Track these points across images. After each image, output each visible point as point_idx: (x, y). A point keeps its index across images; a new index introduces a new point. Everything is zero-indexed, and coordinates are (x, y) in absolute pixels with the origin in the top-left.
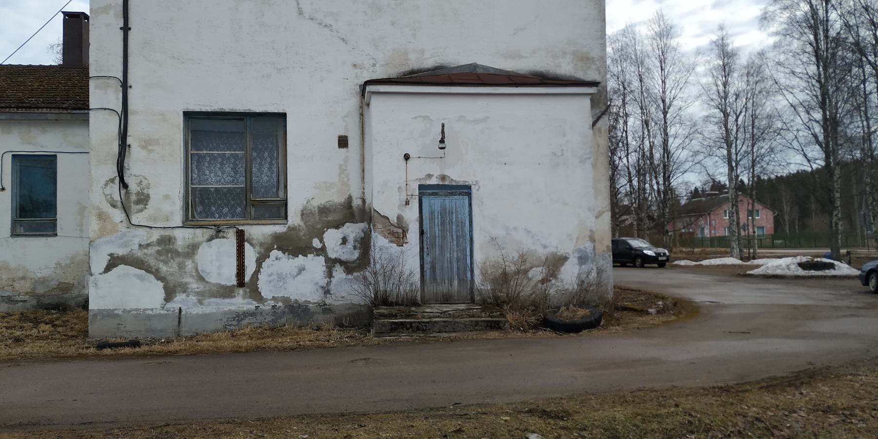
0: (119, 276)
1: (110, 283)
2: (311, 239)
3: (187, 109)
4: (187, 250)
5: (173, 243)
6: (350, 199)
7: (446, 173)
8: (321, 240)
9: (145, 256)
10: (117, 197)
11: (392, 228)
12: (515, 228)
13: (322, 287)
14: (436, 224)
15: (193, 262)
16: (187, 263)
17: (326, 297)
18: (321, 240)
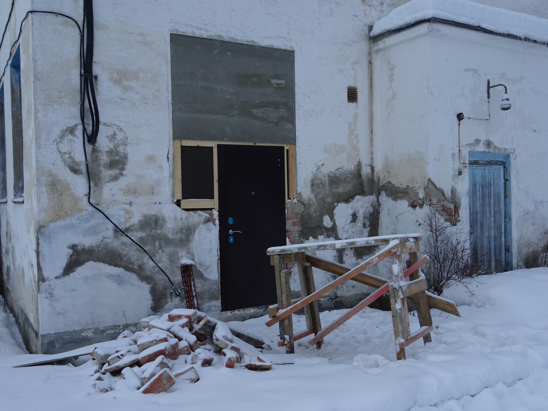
0: (86, 279)
1: (73, 290)
2: (322, 216)
3: (176, 30)
4: (179, 235)
5: (162, 227)
6: (359, 164)
7: (491, 139)
8: (332, 218)
9: (123, 247)
10: (79, 157)
11: (446, 203)
12: (541, 202)
14: (478, 197)
16: (180, 255)
18: (332, 218)
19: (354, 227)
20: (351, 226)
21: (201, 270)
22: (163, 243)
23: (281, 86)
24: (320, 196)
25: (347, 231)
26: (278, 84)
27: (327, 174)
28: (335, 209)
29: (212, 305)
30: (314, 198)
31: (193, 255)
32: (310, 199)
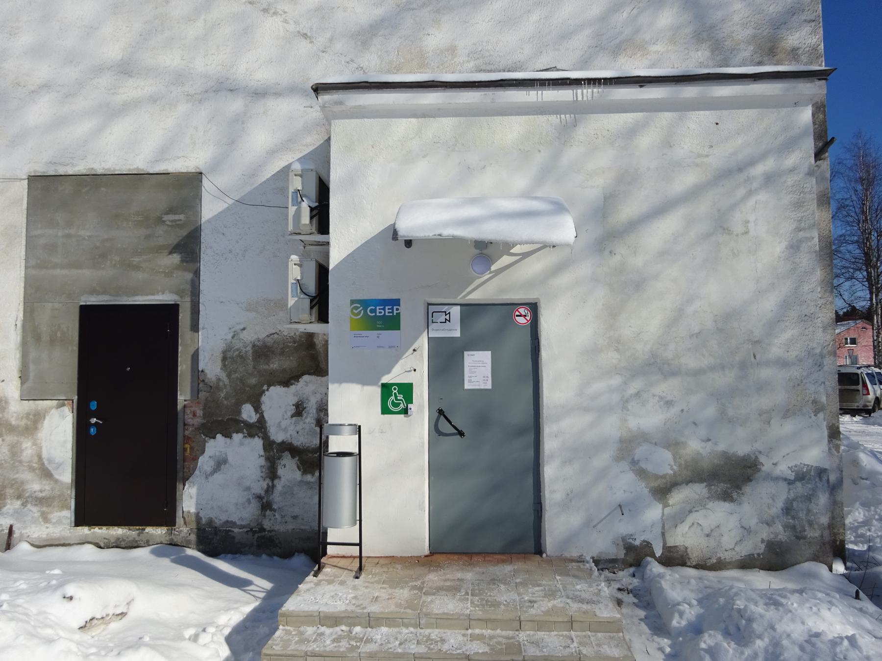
8: (257, 408)
13: (259, 497)
15: (35, 444)
16: (24, 446)
17: (265, 516)
18: (257, 408)
19: (299, 424)
20: (293, 422)
21: (50, 468)
22: (4, 430)
23: (178, 223)
24: (237, 374)
25: (285, 430)
26: (172, 221)
27: (251, 342)
28: (263, 395)
29: (64, 516)
30: (227, 378)
31: (41, 448)
32: (219, 380)
